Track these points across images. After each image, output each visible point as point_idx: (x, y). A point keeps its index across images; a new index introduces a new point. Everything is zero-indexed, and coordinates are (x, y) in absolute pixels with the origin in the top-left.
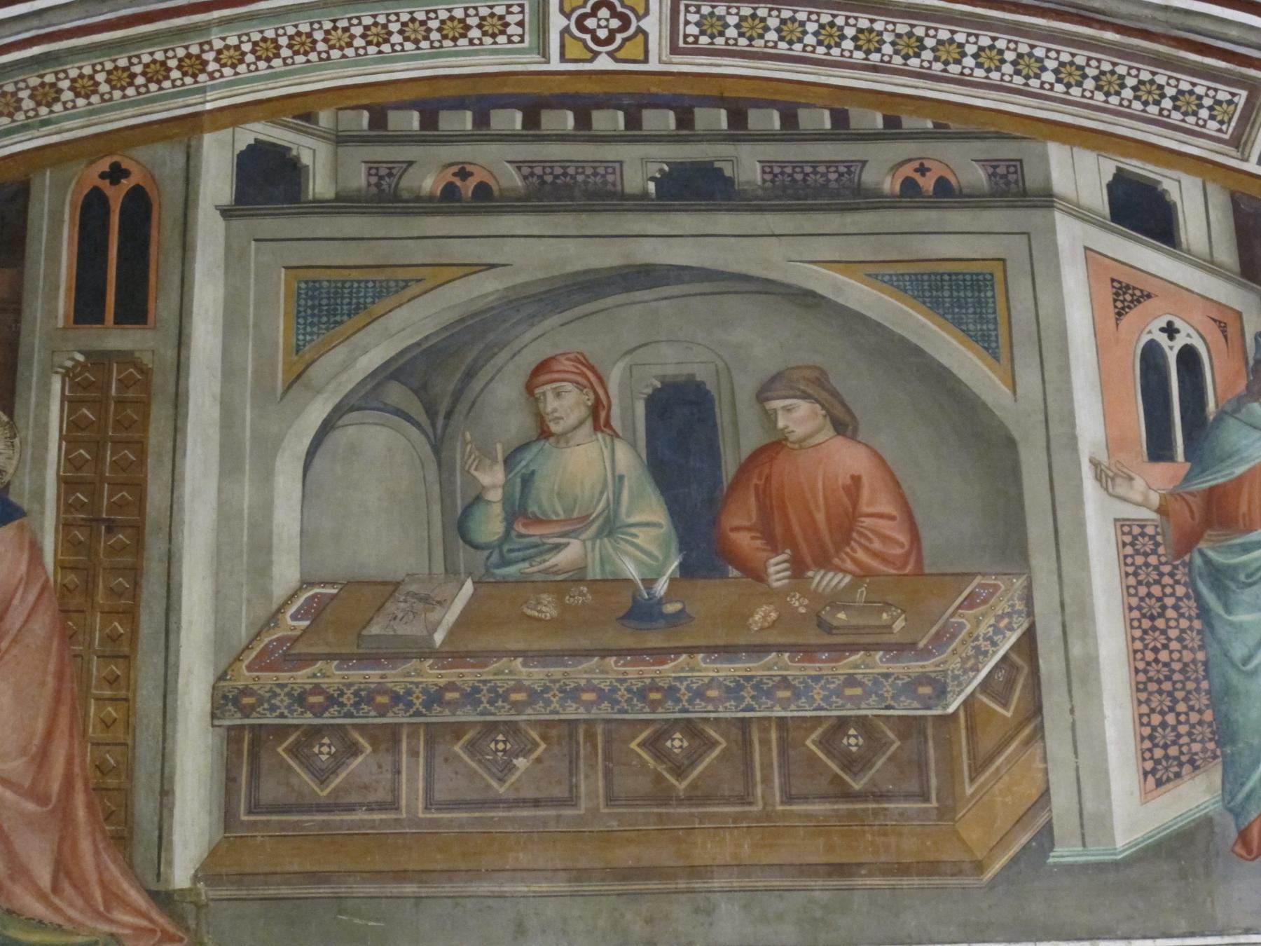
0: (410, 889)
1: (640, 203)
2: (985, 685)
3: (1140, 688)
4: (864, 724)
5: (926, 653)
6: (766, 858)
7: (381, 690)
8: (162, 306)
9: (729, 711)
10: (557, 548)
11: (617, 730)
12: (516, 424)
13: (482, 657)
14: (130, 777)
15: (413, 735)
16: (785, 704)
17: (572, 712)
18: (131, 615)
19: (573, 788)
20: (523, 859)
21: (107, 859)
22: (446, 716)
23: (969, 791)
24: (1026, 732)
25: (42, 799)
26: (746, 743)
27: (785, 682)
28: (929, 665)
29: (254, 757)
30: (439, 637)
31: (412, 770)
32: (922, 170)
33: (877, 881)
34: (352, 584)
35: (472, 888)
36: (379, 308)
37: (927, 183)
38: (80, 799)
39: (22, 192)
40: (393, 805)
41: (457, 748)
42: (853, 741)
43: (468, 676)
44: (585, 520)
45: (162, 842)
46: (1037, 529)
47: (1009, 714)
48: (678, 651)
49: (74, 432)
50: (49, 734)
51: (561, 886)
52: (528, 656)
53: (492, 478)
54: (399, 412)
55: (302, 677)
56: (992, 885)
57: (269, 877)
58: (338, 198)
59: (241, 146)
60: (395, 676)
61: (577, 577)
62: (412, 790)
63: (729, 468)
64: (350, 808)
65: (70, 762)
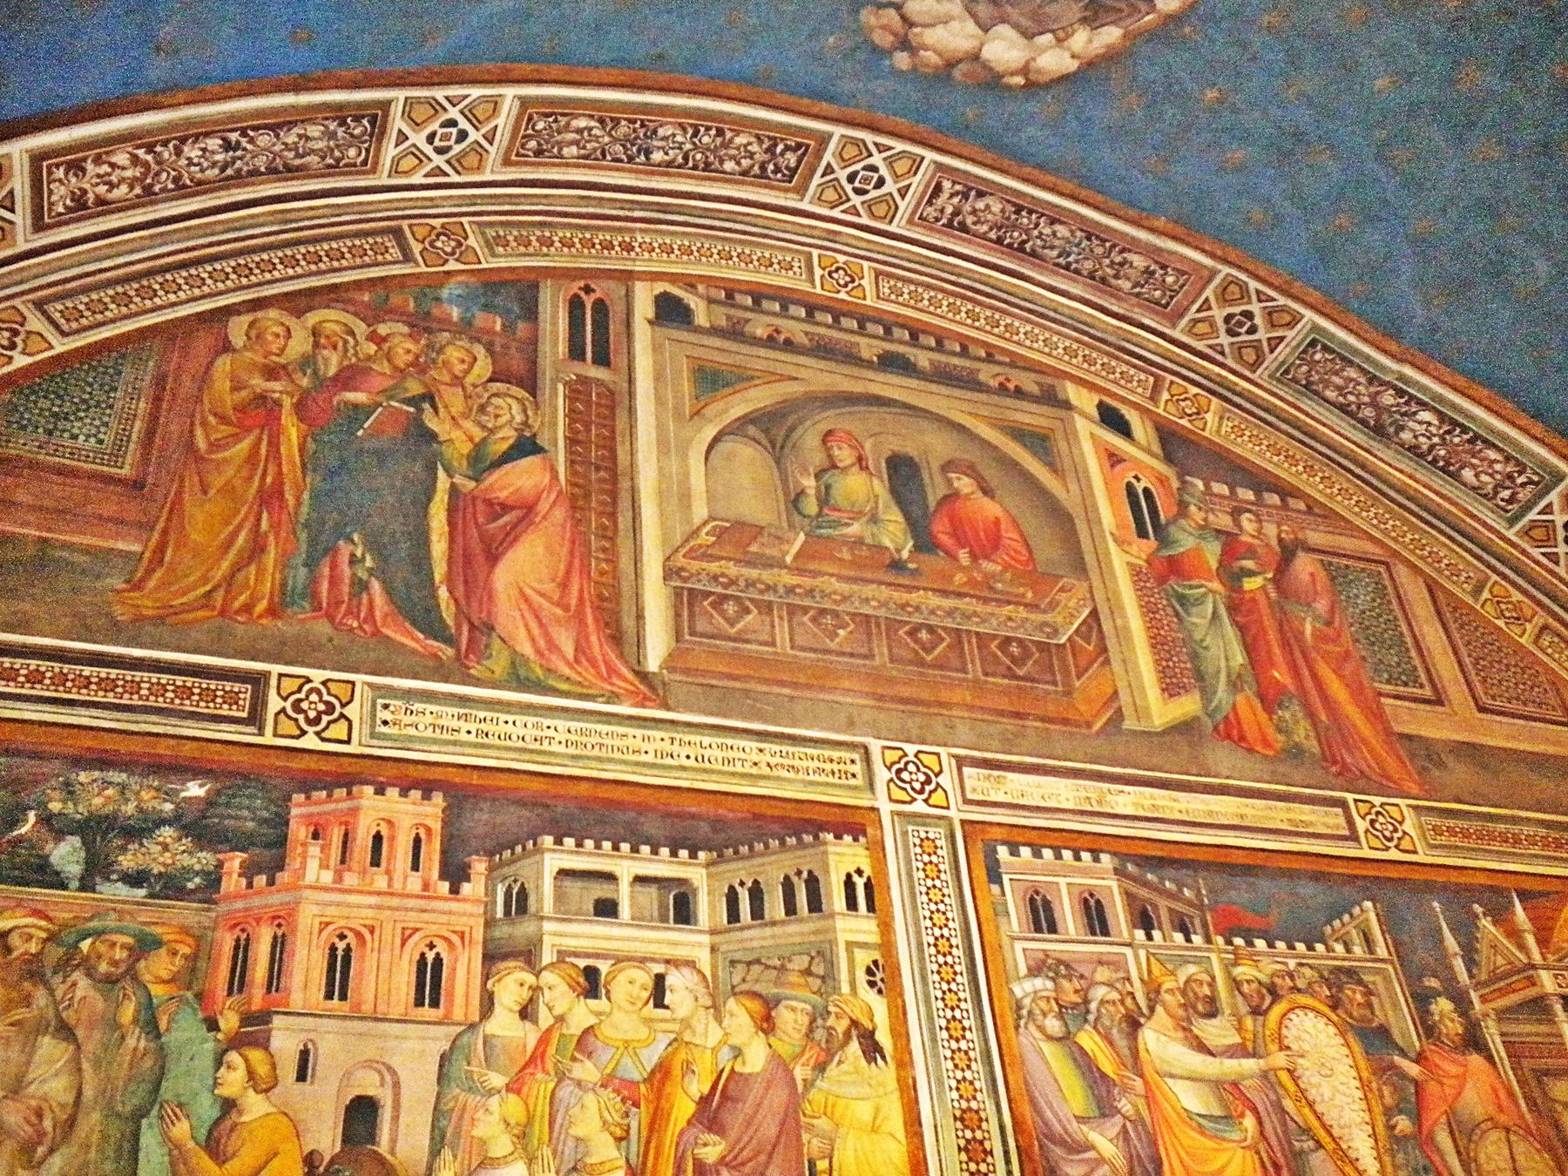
0: (786, 691)
1: (868, 364)
2: (1077, 631)
3: (1153, 646)
4: (1020, 642)
5: (1045, 612)
6: (977, 703)
7: (760, 580)
8: (619, 360)
9: (949, 623)
10: (847, 525)
11: (892, 625)
12: (818, 459)
13: (815, 574)
14: (618, 604)
15: (780, 609)
16: (977, 624)
17: (866, 610)
18: (613, 516)
19: (871, 650)
20: (847, 684)
21: (607, 648)
22: (798, 601)
23: (1077, 684)
24: (1101, 659)
25: (566, 608)
26: (960, 642)
27: (975, 614)
28: (1048, 617)
29: (691, 606)
30: (789, 559)
31: (781, 626)
32: (1008, 380)
33: (1038, 724)
34: (739, 525)
35: (821, 696)
36: (737, 387)
37: (1011, 386)
38: (589, 611)
39: (535, 287)
40: (773, 644)
41: (805, 619)
42: (1014, 649)
43: (808, 582)
44: (861, 513)
45: (640, 643)
46: (1089, 558)
47: (1091, 648)
48: (918, 589)
49: (572, 414)
50: (568, 572)
51: (872, 702)
52: (840, 578)
53: (809, 483)
54: (754, 439)
55: (714, 567)
56: (1098, 733)
57: (704, 673)
58: (712, 327)
59: (657, 292)
60: (767, 576)
61: (859, 541)
62: (783, 638)
63: (932, 501)
64: (747, 641)
65: (581, 591)
